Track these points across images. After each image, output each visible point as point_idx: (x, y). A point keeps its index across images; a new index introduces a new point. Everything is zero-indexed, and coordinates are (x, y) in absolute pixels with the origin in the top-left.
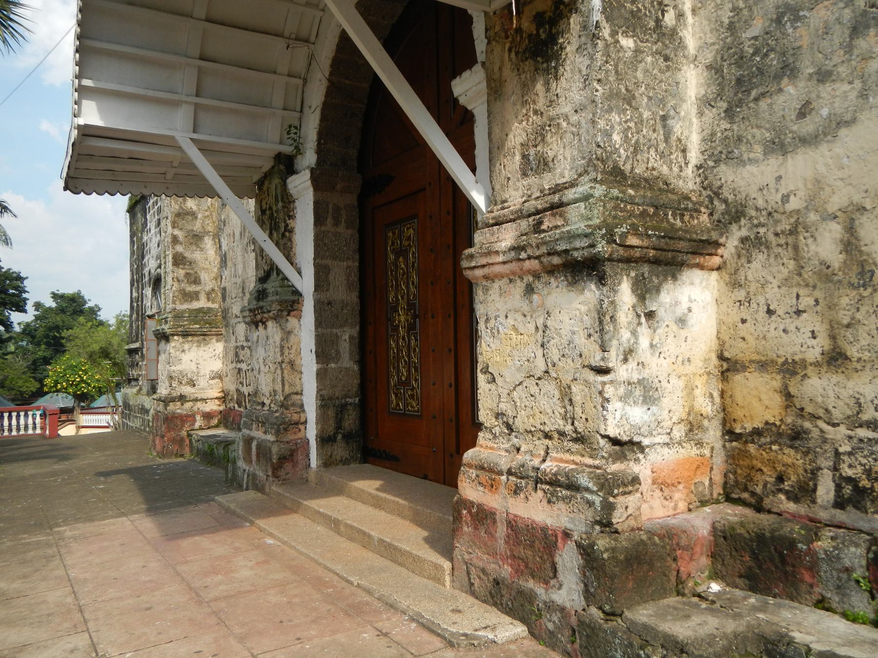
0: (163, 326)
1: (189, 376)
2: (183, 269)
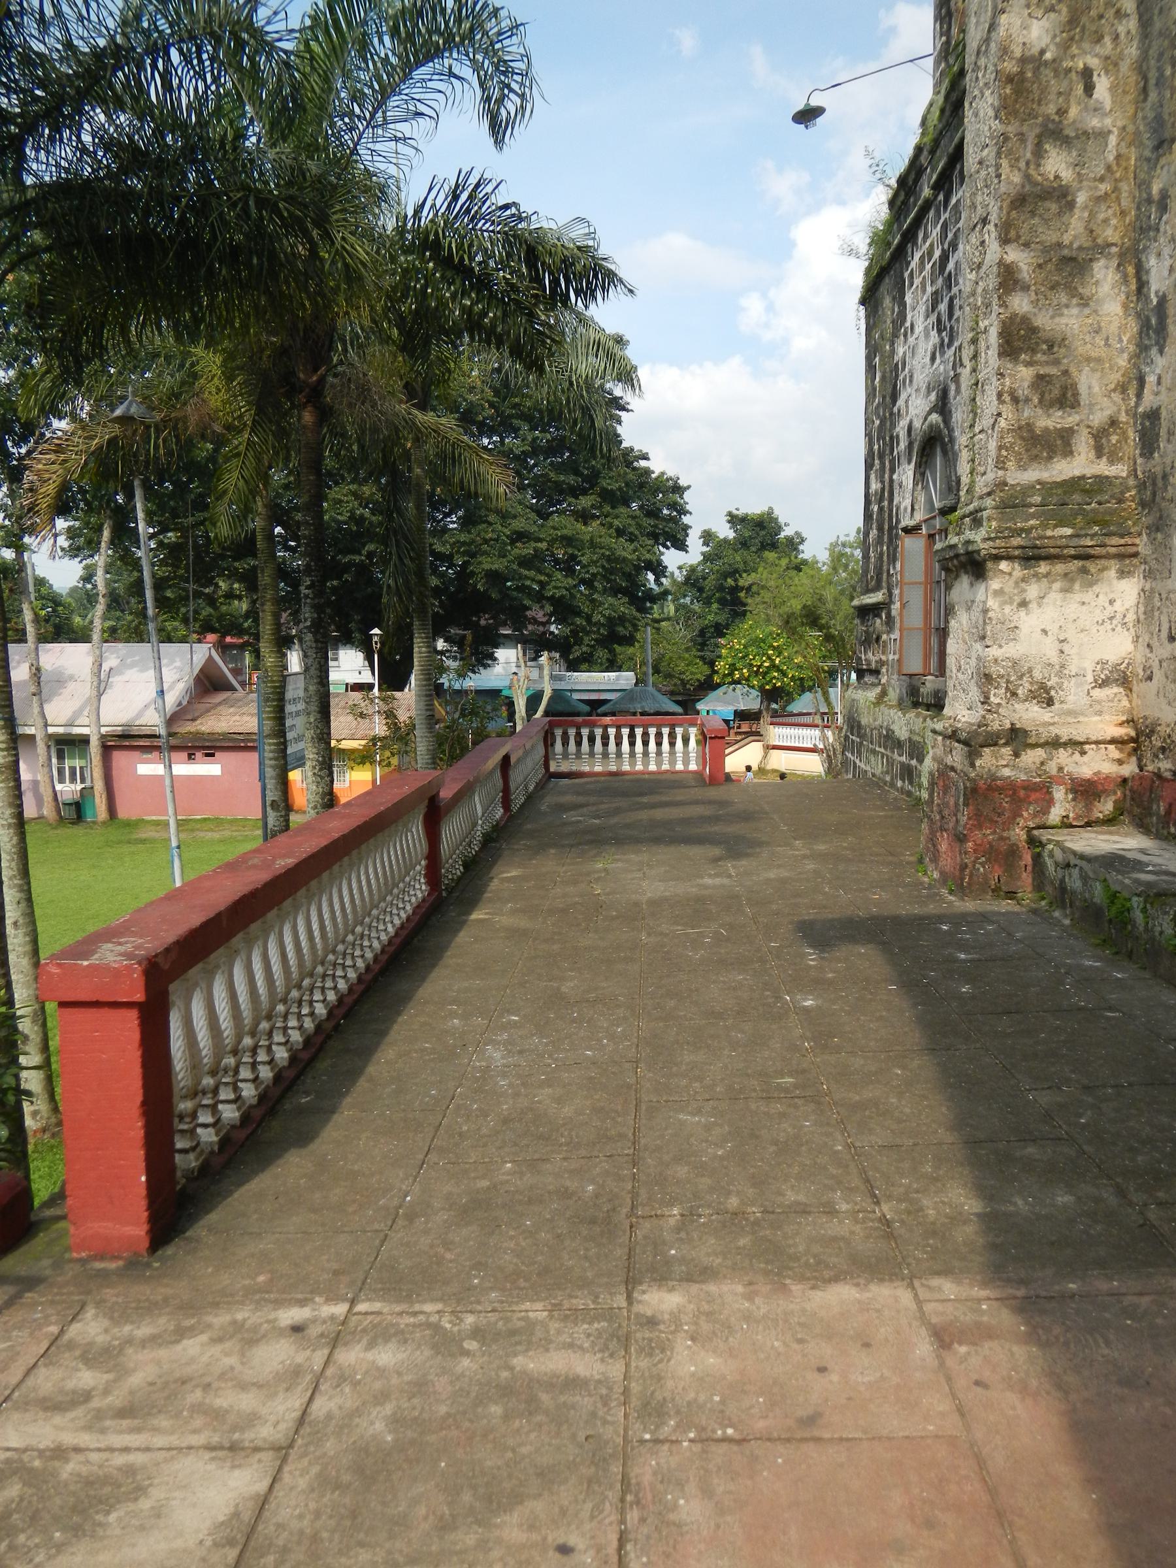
0: (969, 535)
1: (1037, 675)
2: (1028, 364)
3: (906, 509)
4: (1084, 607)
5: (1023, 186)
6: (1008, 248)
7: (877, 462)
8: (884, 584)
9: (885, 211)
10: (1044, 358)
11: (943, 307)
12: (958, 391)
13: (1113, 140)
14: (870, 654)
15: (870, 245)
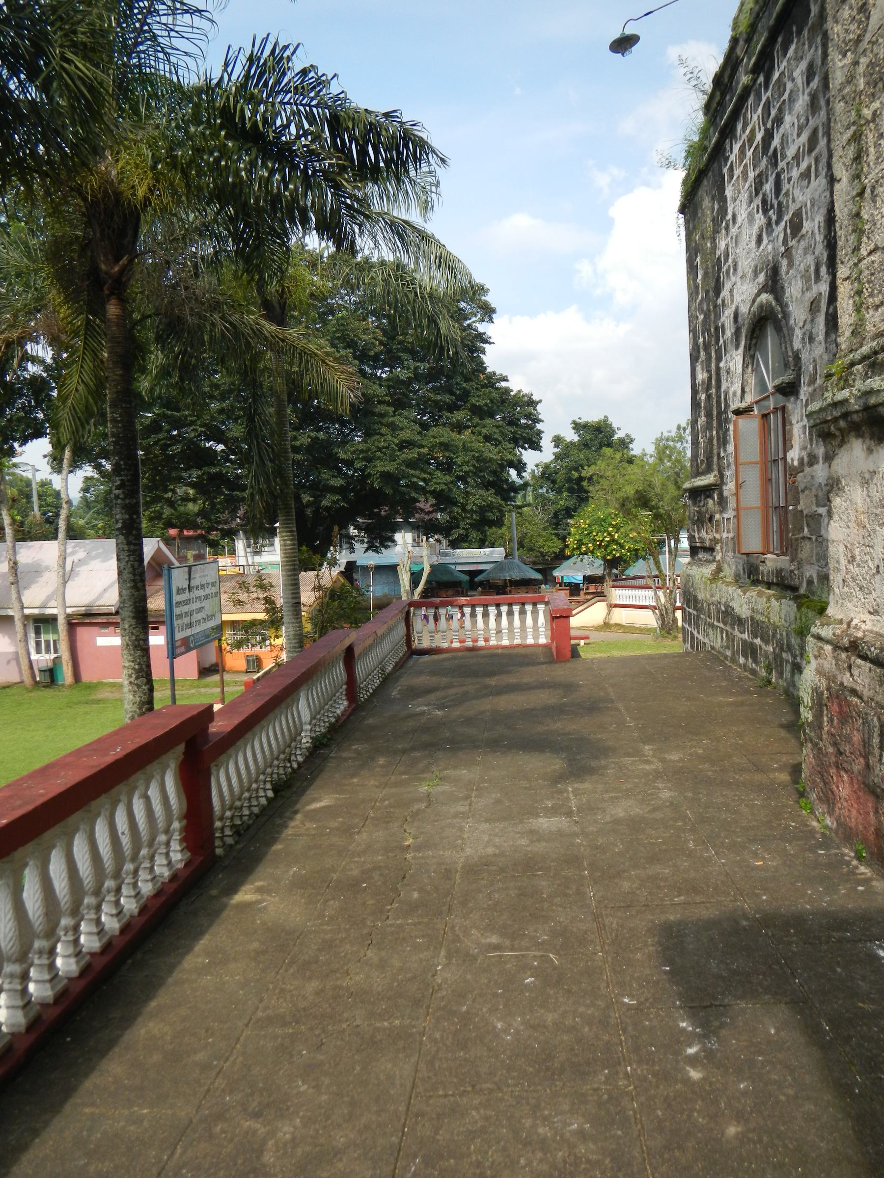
3: (735, 394)
7: (702, 353)
8: (715, 467)
9: (700, 118)
11: (768, 187)
12: (791, 265)
15: (686, 158)
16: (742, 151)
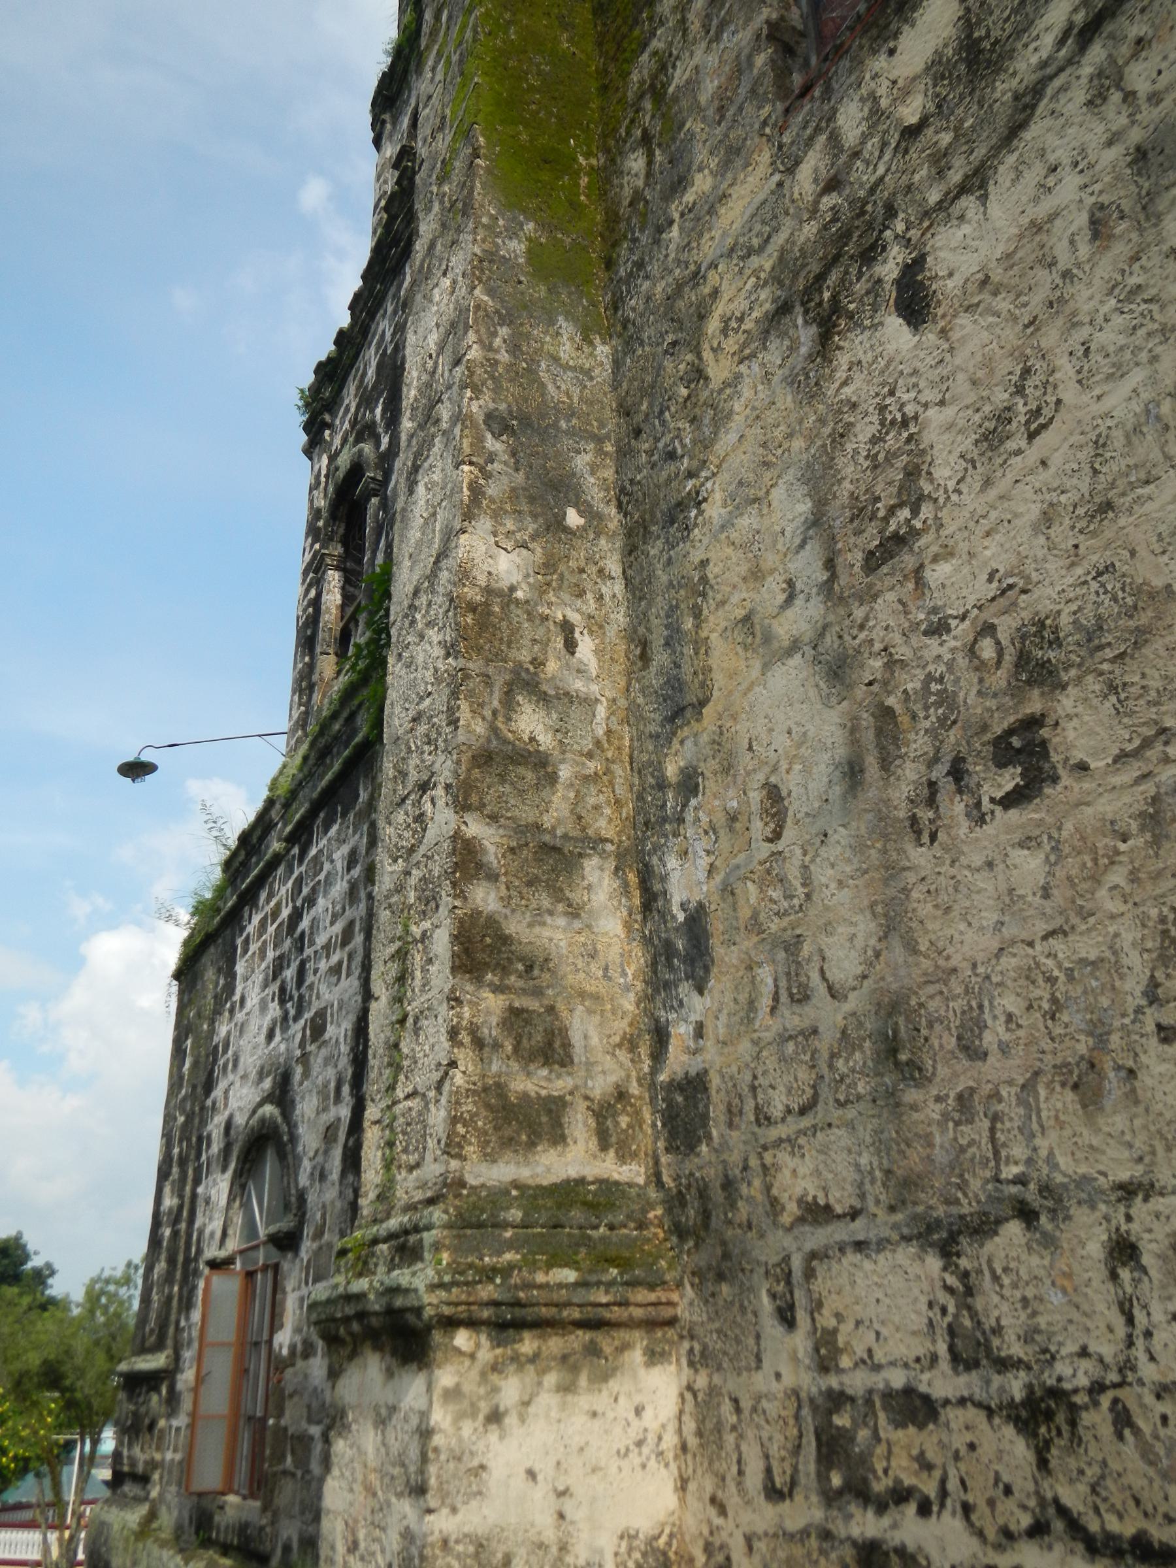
0: (402, 1277)
2: (497, 989)
3: (212, 1235)
4: (597, 1424)
5: (489, 741)
6: (468, 817)
7: (175, 1170)
8: (169, 1342)
9: (217, 874)
10: (520, 984)
11: (289, 973)
12: (306, 1074)
13: (601, 711)
14: (137, 1451)
15: (193, 915)
16: (263, 925)
